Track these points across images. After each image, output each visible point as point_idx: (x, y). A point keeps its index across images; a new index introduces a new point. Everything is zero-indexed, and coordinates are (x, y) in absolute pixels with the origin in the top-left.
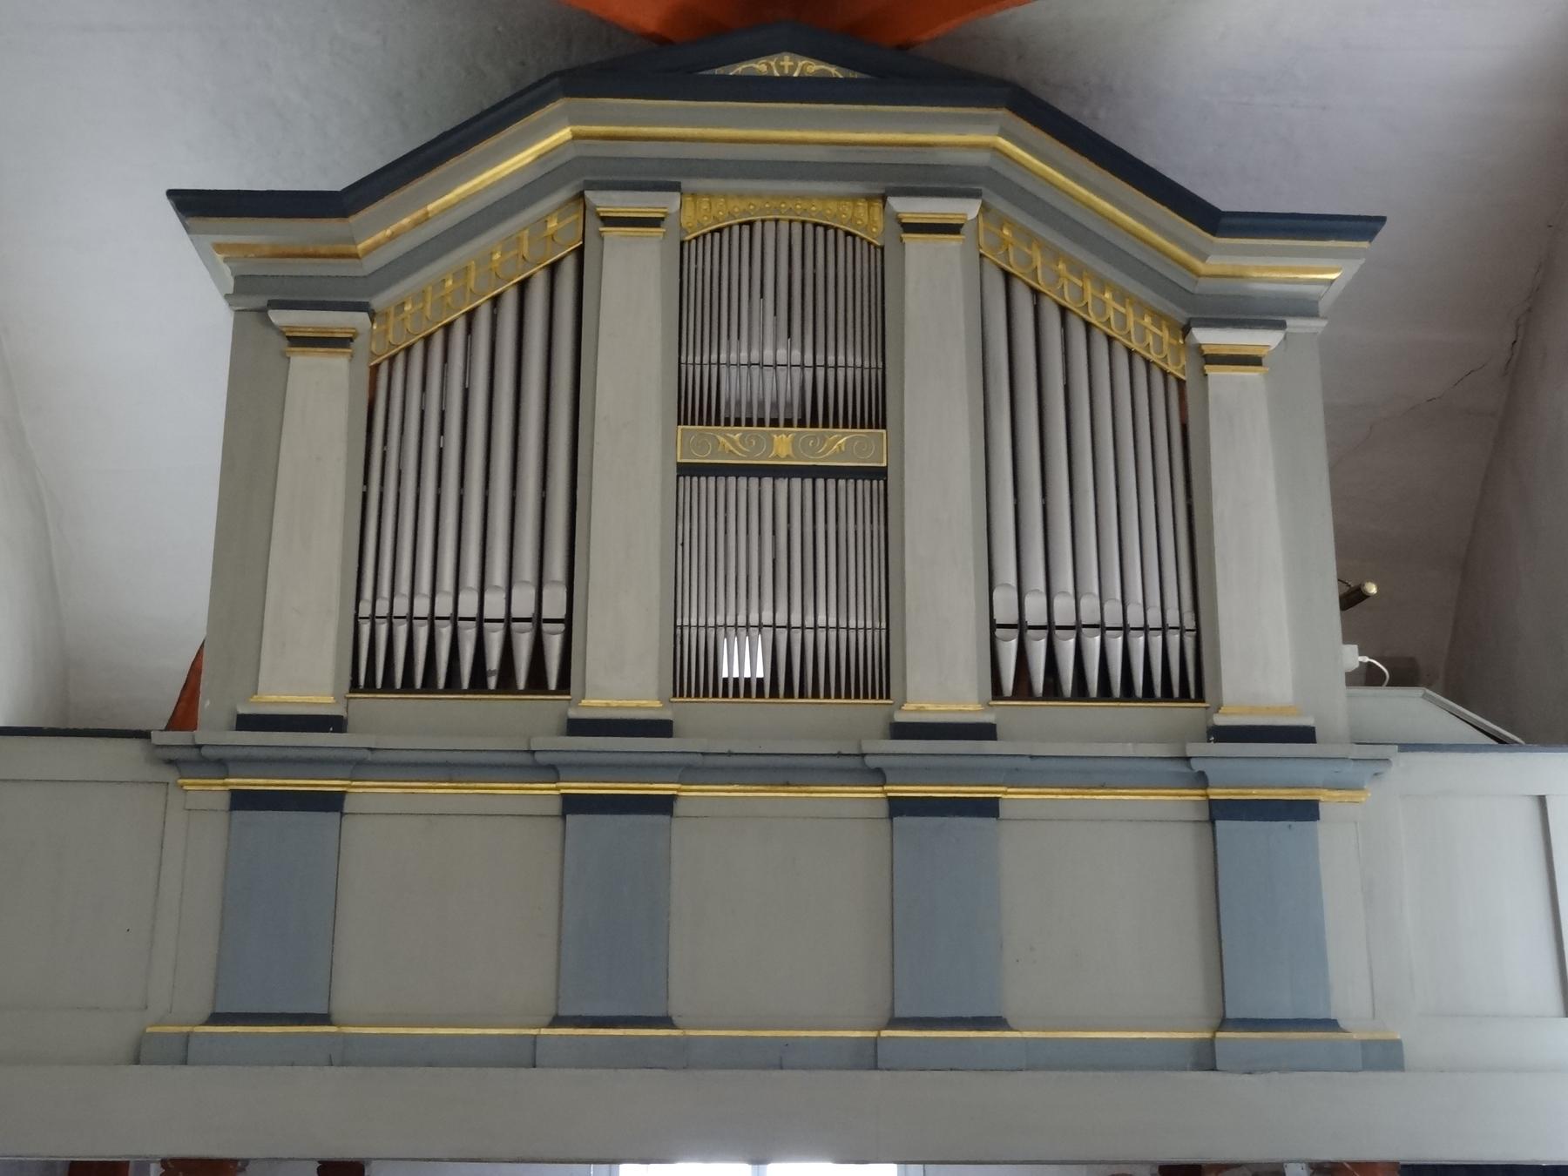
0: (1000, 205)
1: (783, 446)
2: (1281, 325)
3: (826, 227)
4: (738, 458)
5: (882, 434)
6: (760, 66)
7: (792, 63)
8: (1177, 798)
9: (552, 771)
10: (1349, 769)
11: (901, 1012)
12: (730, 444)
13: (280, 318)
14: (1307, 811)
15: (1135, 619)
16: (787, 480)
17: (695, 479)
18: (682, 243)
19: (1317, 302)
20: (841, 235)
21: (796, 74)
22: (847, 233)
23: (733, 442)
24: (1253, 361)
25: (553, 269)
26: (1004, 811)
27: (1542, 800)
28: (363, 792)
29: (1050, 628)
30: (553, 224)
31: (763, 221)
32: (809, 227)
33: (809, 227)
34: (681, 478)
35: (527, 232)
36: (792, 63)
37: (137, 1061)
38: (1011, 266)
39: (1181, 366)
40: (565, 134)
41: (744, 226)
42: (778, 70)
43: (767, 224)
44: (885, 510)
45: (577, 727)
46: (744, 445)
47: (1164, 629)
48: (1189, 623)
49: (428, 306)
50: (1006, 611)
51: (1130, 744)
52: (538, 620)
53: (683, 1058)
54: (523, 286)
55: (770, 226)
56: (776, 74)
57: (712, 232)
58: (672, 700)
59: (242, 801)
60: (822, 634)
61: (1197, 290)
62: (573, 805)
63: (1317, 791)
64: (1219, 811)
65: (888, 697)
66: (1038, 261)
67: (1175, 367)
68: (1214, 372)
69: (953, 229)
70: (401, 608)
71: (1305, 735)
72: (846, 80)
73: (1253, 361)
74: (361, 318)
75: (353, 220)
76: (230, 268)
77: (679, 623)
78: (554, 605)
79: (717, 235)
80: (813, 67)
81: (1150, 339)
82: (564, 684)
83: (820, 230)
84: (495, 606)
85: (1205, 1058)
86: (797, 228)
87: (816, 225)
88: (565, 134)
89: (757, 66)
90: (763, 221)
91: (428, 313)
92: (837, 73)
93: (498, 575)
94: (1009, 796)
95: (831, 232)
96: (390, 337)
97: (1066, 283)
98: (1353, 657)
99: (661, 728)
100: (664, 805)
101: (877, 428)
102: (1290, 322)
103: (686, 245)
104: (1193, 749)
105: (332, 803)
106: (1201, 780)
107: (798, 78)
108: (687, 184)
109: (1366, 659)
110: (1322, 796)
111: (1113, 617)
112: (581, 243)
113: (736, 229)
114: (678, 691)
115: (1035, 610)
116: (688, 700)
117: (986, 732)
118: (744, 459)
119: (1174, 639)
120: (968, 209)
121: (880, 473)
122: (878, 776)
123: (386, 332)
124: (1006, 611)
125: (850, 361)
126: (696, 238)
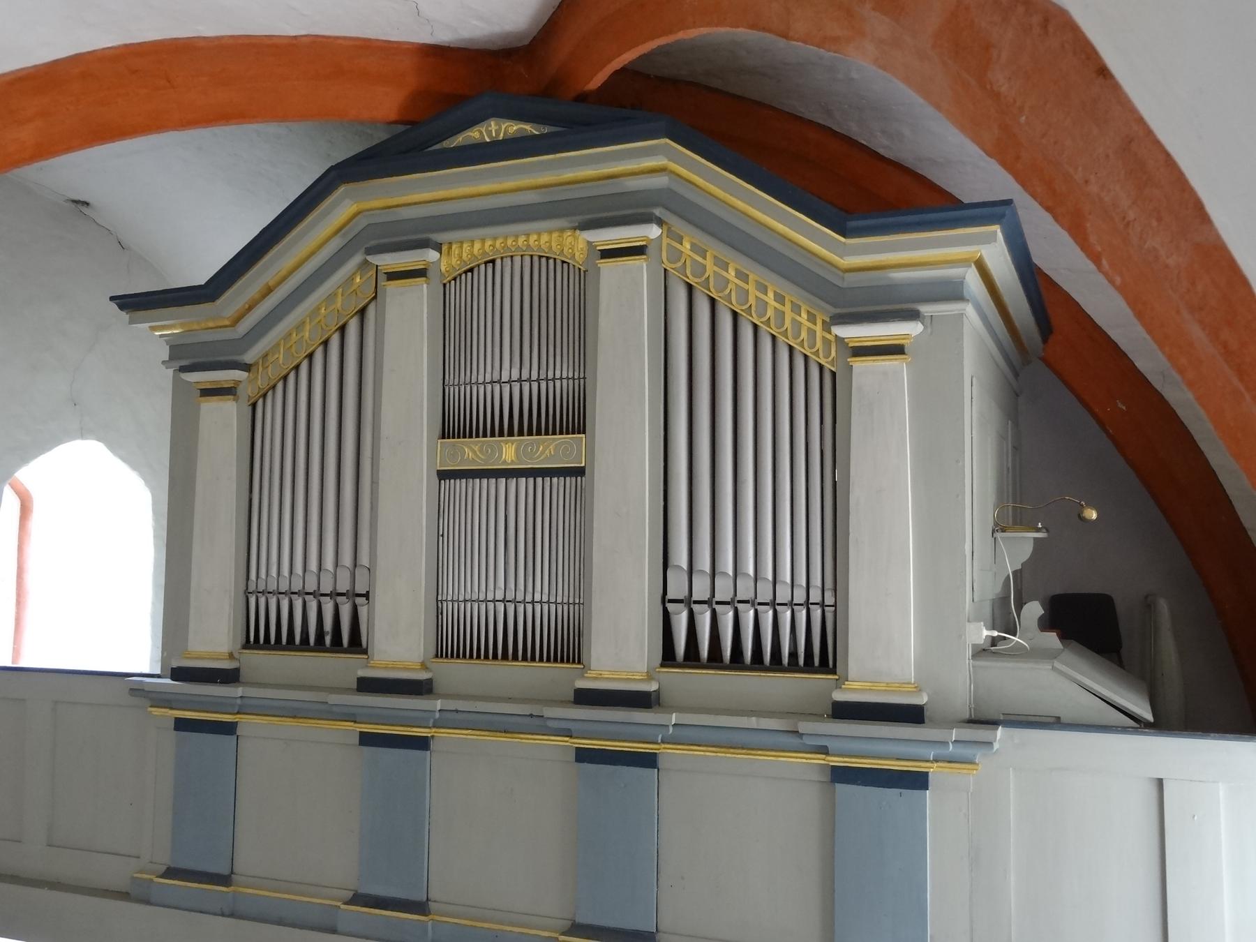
1: (509, 452)
2: (913, 315)
3: (548, 258)
4: (481, 465)
5: (582, 438)
6: (475, 134)
7: (497, 127)
8: (804, 761)
12: (472, 452)
14: (918, 781)
15: (783, 595)
16: (515, 479)
17: (448, 481)
18: (445, 285)
19: (962, 283)
20: (559, 263)
21: (501, 138)
22: (563, 262)
23: (474, 452)
24: (896, 350)
26: (662, 763)
27: (1160, 782)
31: (502, 258)
32: (536, 259)
33: (536, 259)
34: (443, 482)
35: (341, 289)
36: (497, 127)
38: (688, 278)
39: (830, 359)
41: (488, 264)
42: (489, 137)
43: (505, 259)
44: (581, 504)
46: (483, 455)
47: (807, 604)
48: (829, 600)
49: (281, 356)
51: (753, 718)
55: (508, 261)
56: (488, 140)
57: (466, 272)
58: (434, 660)
60: (538, 607)
61: (845, 285)
63: (928, 764)
64: (841, 775)
65: (579, 662)
67: (826, 360)
68: (861, 365)
69: (638, 251)
71: (912, 715)
72: (542, 136)
73: (896, 350)
75: (218, 302)
77: (440, 598)
79: (469, 274)
81: (804, 335)
83: (544, 260)
86: (527, 259)
87: (540, 257)
89: (471, 134)
90: (502, 258)
91: (281, 362)
92: (532, 130)
95: (551, 261)
96: (259, 382)
97: (734, 287)
101: (579, 433)
102: (925, 309)
103: (448, 285)
105: (228, 729)
107: (503, 139)
108: (438, 237)
109: (996, 634)
110: (933, 769)
111: (765, 594)
112: (374, 294)
113: (483, 267)
115: (701, 589)
116: (445, 661)
118: (481, 465)
119: (817, 613)
120: (654, 231)
121: (579, 472)
123: (256, 378)
126: (455, 279)
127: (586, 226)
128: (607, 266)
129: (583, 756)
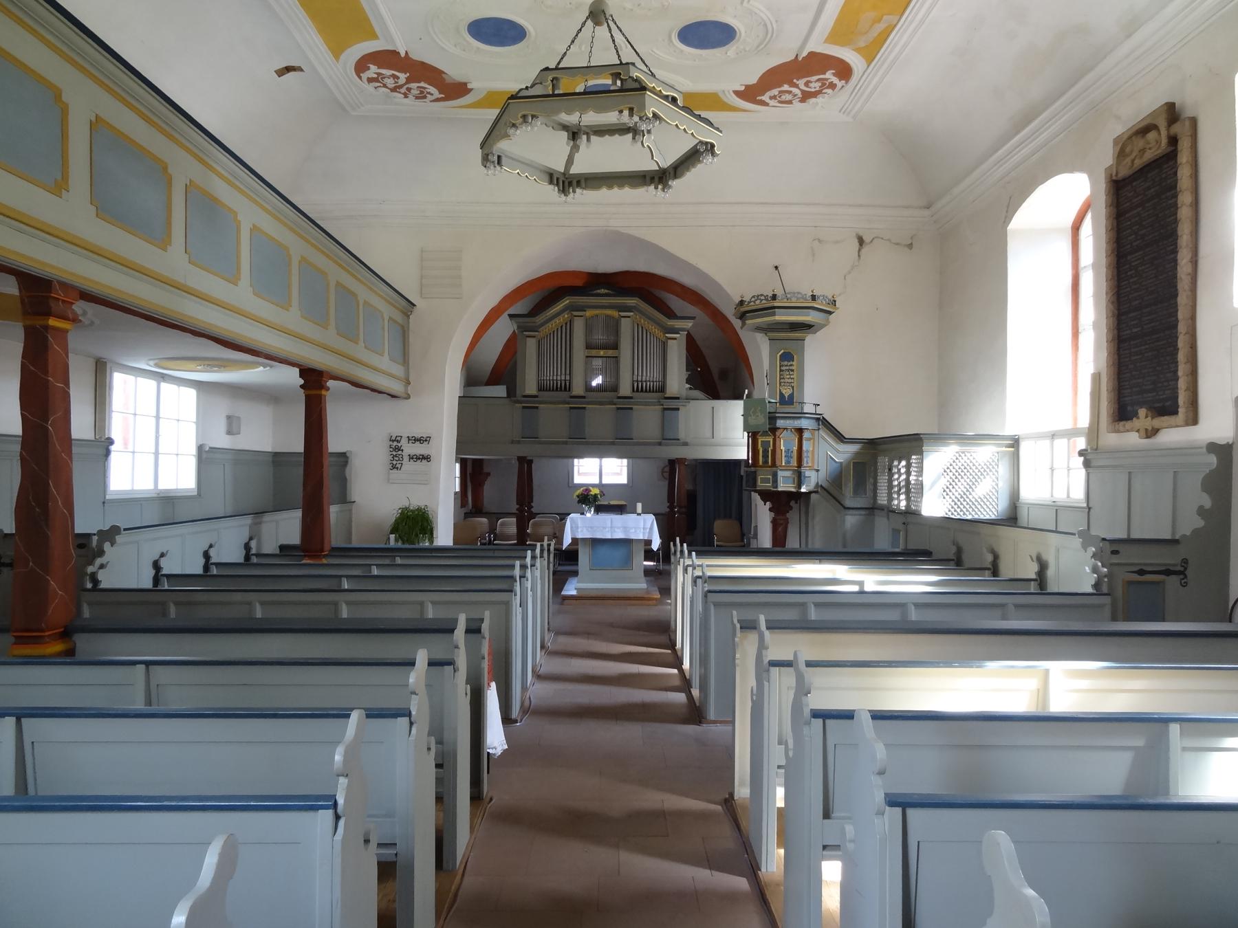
1: (602, 353)
9: (568, 403)
10: (684, 404)
12: (594, 352)
13: (525, 333)
14: (678, 409)
15: (655, 380)
24: (675, 339)
25: (566, 324)
28: (541, 406)
30: (566, 316)
37: (512, 443)
40: (568, 301)
45: (572, 397)
47: (659, 382)
50: (635, 379)
52: (565, 380)
53: (587, 443)
54: (562, 327)
59: (524, 407)
62: (571, 408)
64: (665, 409)
66: (642, 321)
68: (669, 341)
71: (678, 398)
73: (675, 339)
74: (537, 333)
76: (517, 323)
78: (568, 378)
80: (606, 291)
82: (569, 390)
85: (660, 444)
88: (568, 301)
93: (559, 374)
94: (634, 407)
98: (688, 386)
99: (584, 397)
100: (584, 408)
104: (661, 400)
106: (662, 405)
108: (586, 309)
114: (586, 391)
115: (640, 379)
117: (631, 398)
120: (632, 314)
121: (616, 357)
122: (615, 404)
124: (635, 379)
125: (612, 338)
127: (619, 311)
128: (622, 319)
129: (618, 409)
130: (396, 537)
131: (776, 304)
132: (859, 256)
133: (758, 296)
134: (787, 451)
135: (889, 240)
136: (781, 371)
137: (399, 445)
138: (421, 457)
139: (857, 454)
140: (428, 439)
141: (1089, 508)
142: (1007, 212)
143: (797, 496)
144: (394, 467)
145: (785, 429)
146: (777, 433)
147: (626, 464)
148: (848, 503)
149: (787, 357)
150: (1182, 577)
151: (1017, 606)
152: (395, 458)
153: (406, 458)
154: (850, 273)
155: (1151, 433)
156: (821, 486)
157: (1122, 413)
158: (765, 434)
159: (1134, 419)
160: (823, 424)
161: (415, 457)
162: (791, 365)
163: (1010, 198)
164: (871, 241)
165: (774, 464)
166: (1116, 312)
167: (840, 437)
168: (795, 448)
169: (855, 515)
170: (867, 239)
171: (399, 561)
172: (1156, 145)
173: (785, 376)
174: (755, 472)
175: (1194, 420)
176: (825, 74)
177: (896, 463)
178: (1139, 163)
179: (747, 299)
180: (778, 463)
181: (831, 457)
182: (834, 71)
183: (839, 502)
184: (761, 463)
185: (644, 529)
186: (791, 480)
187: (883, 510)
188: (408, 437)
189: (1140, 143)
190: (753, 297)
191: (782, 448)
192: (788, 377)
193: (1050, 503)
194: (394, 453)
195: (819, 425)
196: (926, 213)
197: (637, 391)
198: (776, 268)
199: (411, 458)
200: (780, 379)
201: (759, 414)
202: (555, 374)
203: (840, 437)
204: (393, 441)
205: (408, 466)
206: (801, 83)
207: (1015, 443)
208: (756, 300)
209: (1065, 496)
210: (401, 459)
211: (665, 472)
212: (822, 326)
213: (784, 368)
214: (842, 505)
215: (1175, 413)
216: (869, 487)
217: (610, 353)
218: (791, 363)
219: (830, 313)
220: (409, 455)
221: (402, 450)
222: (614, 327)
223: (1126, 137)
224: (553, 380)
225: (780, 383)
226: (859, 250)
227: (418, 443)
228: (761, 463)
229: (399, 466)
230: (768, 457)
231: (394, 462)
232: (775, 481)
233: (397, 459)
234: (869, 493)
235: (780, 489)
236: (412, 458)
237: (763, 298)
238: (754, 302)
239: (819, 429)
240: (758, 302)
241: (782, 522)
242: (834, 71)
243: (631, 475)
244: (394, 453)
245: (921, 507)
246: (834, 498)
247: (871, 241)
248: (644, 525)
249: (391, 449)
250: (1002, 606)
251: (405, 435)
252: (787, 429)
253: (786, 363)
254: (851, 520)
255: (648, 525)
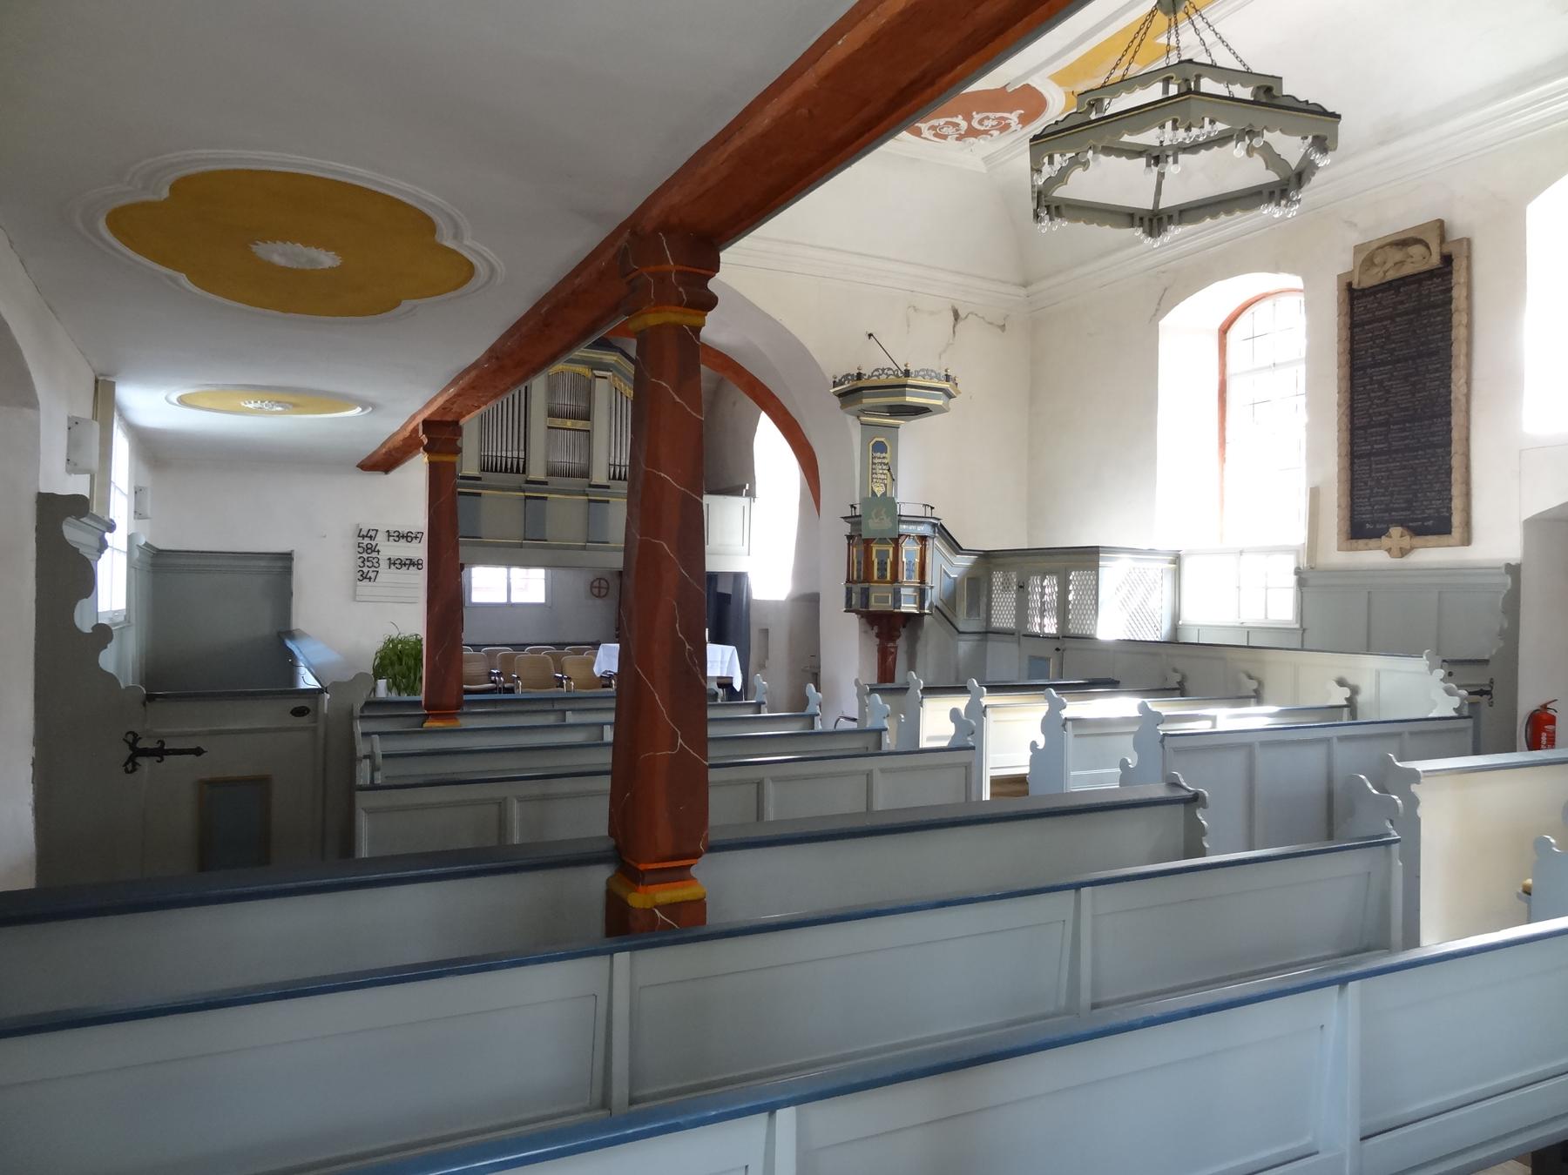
0: (616, 373)
1: (569, 423)
11: (590, 540)
12: (558, 422)
29: (620, 466)
45: (528, 482)
52: (518, 458)
69: (605, 378)
70: (494, 454)
78: (522, 455)
82: (524, 472)
84: (509, 454)
93: (510, 448)
99: (545, 483)
100: (545, 498)
105: (479, 495)
117: (608, 487)
120: (611, 374)
121: (589, 431)
122: (587, 495)
125: (583, 405)
130: (388, 682)
131: (910, 381)
132: (954, 332)
133: (883, 370)
134: (909, 563)
135: (983, 318)
136: (873, 464)
137: (374, 543)
138: (408, 562)
139: (971, 568)
140: (419, 535)
141: (1304, 630)
142: (1159, 304)
143: (913, 620)
144: (364, 577)
145: (907, 536)
146: (900, 541)
147: (500, 572)
148: (962, 628)
149: (880, 447)
150: (1489, 696)
151: (1412, 733)
152: (367, 563)
153: (384, 564)
154: (944, 351)
155: (1403, 553)
156: (936, 607)
157: (1360, 529)
158: (883, 541)
159: (1383, 537)
160: (939, 532)
161: (398, 562)
162: (884, 458)
163: (1165, 290)
164: (966, 317)
165: (895, 578)
166: (1349, 426)
167: (955, 547)
168: (917, 560)
169: (969, 641)
170: (962, 313)
171: (571, 718)
172: (1419, 261)
173: (878, 471)
174: (868, 588)
175: (1467, 540)
176: (1011, 113)
177: (1036, 580)
178: (1391, 275)
179: (866, 371)
180: (900, 578)
181: (945, 572)
182: (1022, 112)
183: (952, 624)
184: (876, 577)
185: (722, 662)
186: (912, 599)
187: (1013, 634)
188: (388, 531)
189: (1397, 255)
190: (877, 370)
191: (904, 560)
192: (881, 471)
193: (1237, 625)
194: (365, 555)
195: (934, 532)
196: (1023, 292)
197: (614, 478)
198: (870, 335)
199: (391, 563)
200: (873, 474)
201: (885, 518)
202: (504, 448)
203: (955, 547)
204: (363, 537)
205: (386, 575)
206: (977, 117)
207: (1177, 559)
208: (880, 375)
209: (1263, 617)
210: (377, 565)
211: (596, 587)
212: (941, 410)
213: (876, 461)
214: (957, 629)
215: (1449, 532)
216: (983, 607)
217: (580, 424)
218: (884, 455)
219: (950, 396)
220: (390, 559)
221: (378, 551)
222: (586, 391)
223: (1375, 246)
224: (497, 456)
225: (873, 478)
226: (954, 326)
227: (403, 541)
228: (876, 577)
229: (372, 575)
230: (886, 570)
231: (365, 570)
232: (897, 599)
233: (370, 564)
234: (983, 615)
235: (903, 610)
236: (394, 564)
237: (890, 372)
238: (878, 376)
239: (935, 537)
240: (884, 377)
241: (893, 650)
242: (1022, 112)
243: (551, 590)
244: (365, 555)
245: (1095, 631)
246: (948, 620)
247: (966, 317)
248: (723, 657)
249: (361, 550)
250: (1399, 734)
251: (382, 529)
252: (910, 536)
253: (878, 454)
254: (964, 647)
255: (727, 658)
